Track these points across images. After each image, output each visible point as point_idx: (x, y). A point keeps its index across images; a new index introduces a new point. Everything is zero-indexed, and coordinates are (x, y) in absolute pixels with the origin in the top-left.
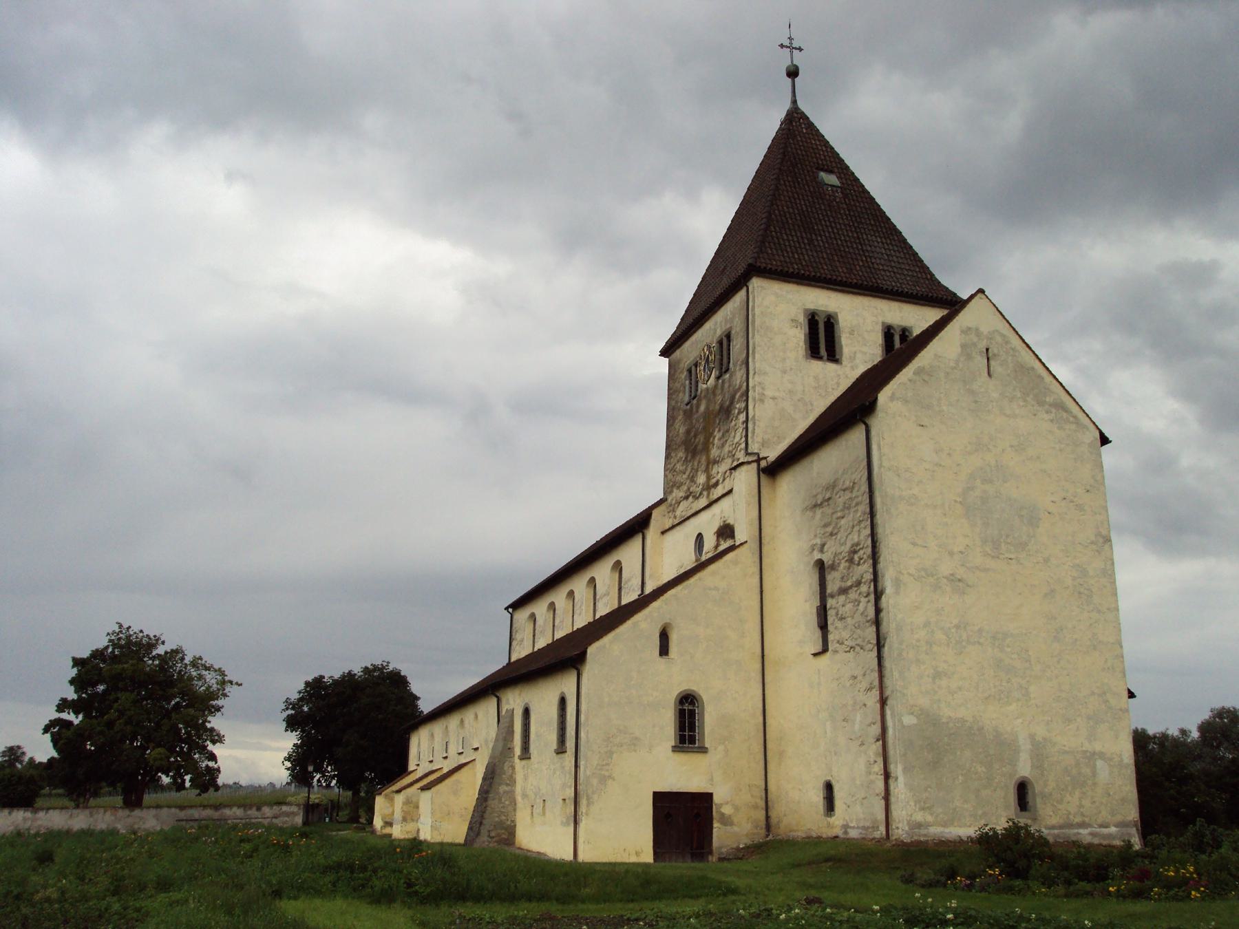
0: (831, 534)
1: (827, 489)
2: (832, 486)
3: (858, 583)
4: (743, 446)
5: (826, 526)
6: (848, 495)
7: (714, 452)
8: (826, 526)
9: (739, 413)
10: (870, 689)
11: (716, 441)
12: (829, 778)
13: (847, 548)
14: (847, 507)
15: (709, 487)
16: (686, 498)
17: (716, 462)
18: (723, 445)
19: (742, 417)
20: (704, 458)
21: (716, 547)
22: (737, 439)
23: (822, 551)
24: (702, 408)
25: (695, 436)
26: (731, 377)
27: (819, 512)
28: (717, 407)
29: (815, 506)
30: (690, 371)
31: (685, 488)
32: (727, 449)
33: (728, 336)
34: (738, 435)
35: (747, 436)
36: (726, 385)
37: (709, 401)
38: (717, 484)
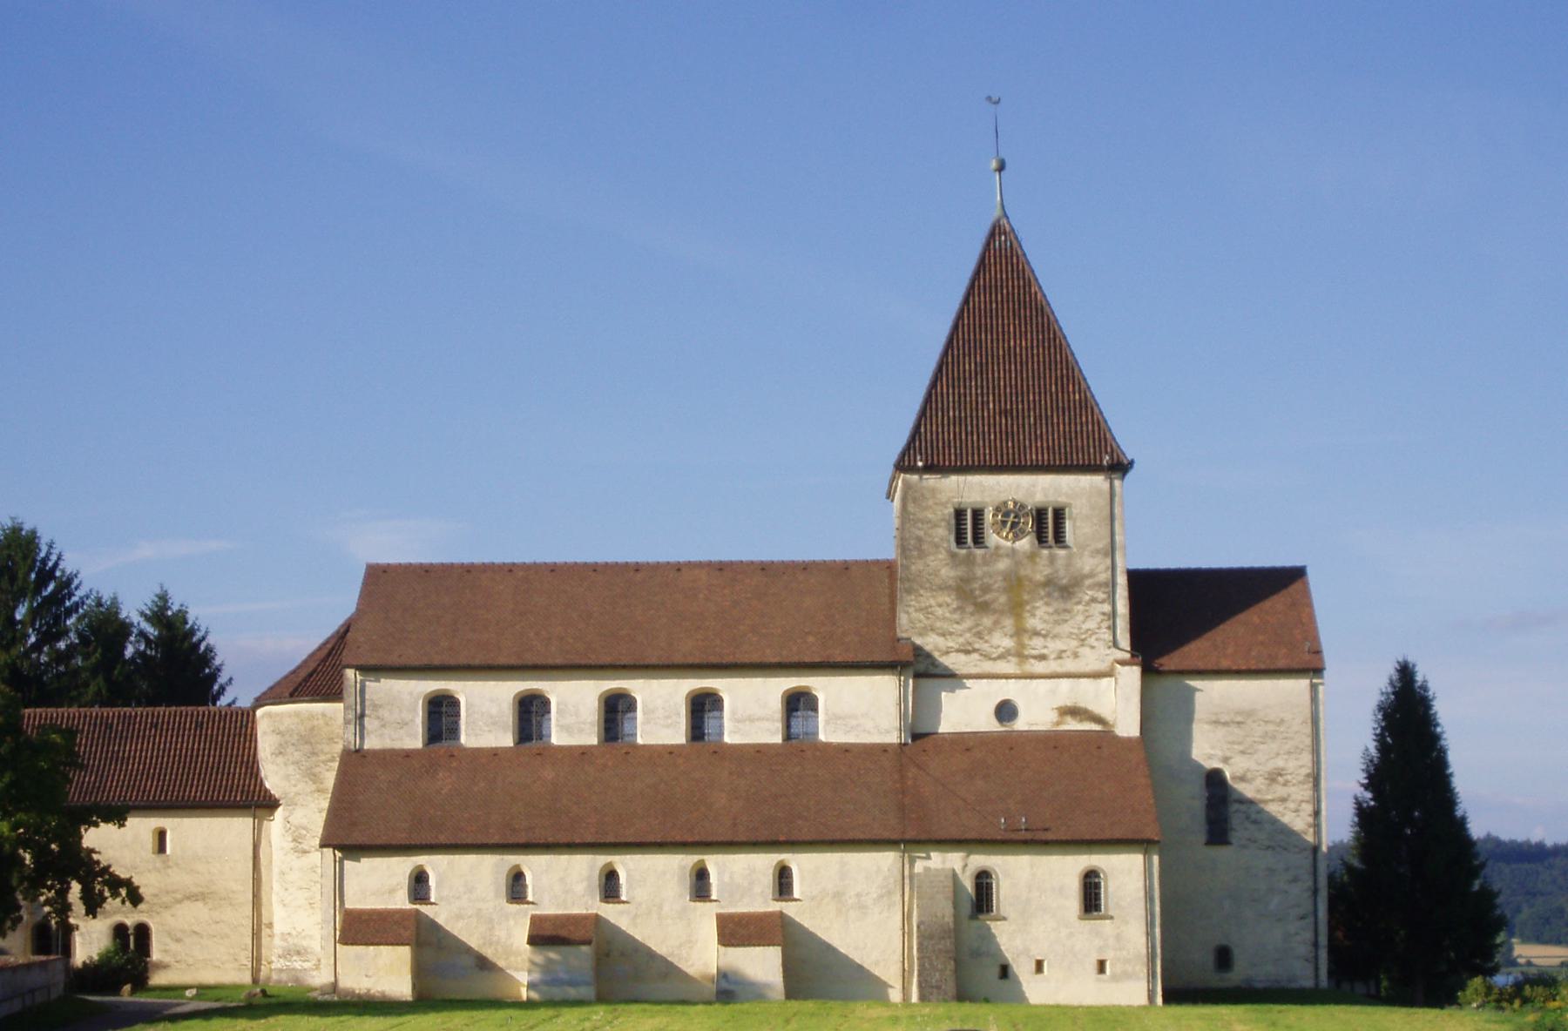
0: (1243, 752)
1: (1238, 713)
2: (1250, 713)
3: (1283, 800)
4: (1108, 636)
5: (1233, 743)
6: (1271, 728)
7: (1033, 622)
8: (1233, 743)
9: (1094, 600)
10: (1295, 880)
11: (1039, 613)
12: (1225, 942)
13: (1271, 766)
14: (1268, 737)
15: (1021, 656)
16: (967, 652)
17: (1037, 633)
18: (1057, 623)
19: (1107, 608)
20: (1008, 623)
21: (1058, 724)
22: (1091, 624)
23: (1226, 760)
24: (1003, 565)
25: (986, 589)
26: (1070, 557)
27: (1221, 732)
28: (1039, 577)
29: (1217, 722)
30: (959, 514)
31: (961, 640)
32: (1066, 629)
33: (1059, 514)
34: (1091, 624)
35: (1113, 628)
36: (1060, 563)
37: (1018, 564)
38: (1042, 657)
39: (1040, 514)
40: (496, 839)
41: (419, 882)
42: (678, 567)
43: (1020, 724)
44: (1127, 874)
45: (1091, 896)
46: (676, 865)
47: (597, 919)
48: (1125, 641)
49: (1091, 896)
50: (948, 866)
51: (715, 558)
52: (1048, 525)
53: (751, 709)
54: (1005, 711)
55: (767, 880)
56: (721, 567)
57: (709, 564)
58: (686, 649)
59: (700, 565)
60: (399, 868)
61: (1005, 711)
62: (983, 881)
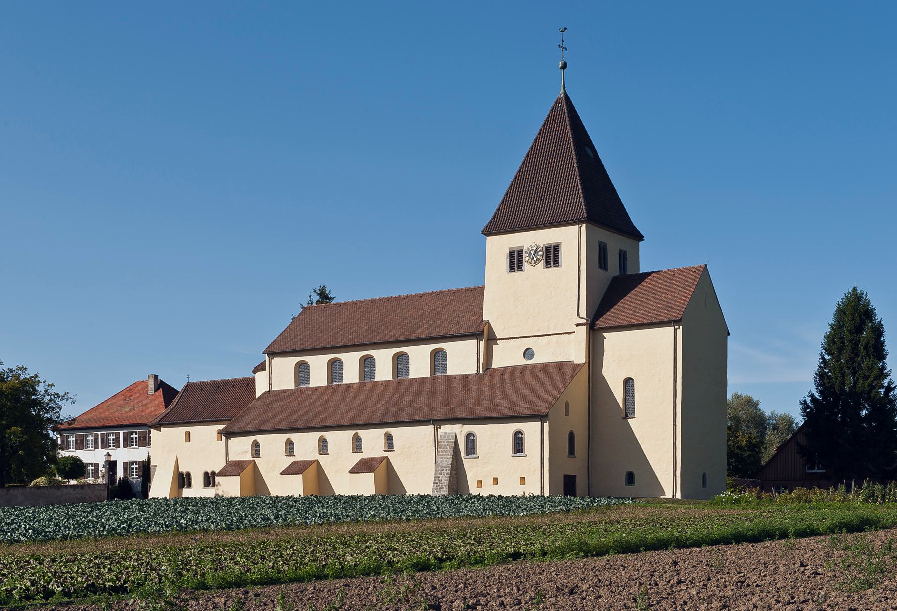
30: (511, 254)
33: (556, 248)
39: (547, 249)
40: (285, 427)
41: (256, 446)
42: (421, 296)
43: (535, 360)
44: (532, 431)
45: (518, 445)
46: (347, 436)
47: (294, 463)
48: (583, 313)
49: (518, 445)
50: (454, 431)
51: (434, 291)
52: (552, 256)
53: (419, 361)
54: (528, 353)
55: (382, 442)
56: (437, 294)
57: (432, 293)
58: (396, 334)
59: (429, 294)
60: (248, 441)
61: (528, 353)
62: (471, 439)
